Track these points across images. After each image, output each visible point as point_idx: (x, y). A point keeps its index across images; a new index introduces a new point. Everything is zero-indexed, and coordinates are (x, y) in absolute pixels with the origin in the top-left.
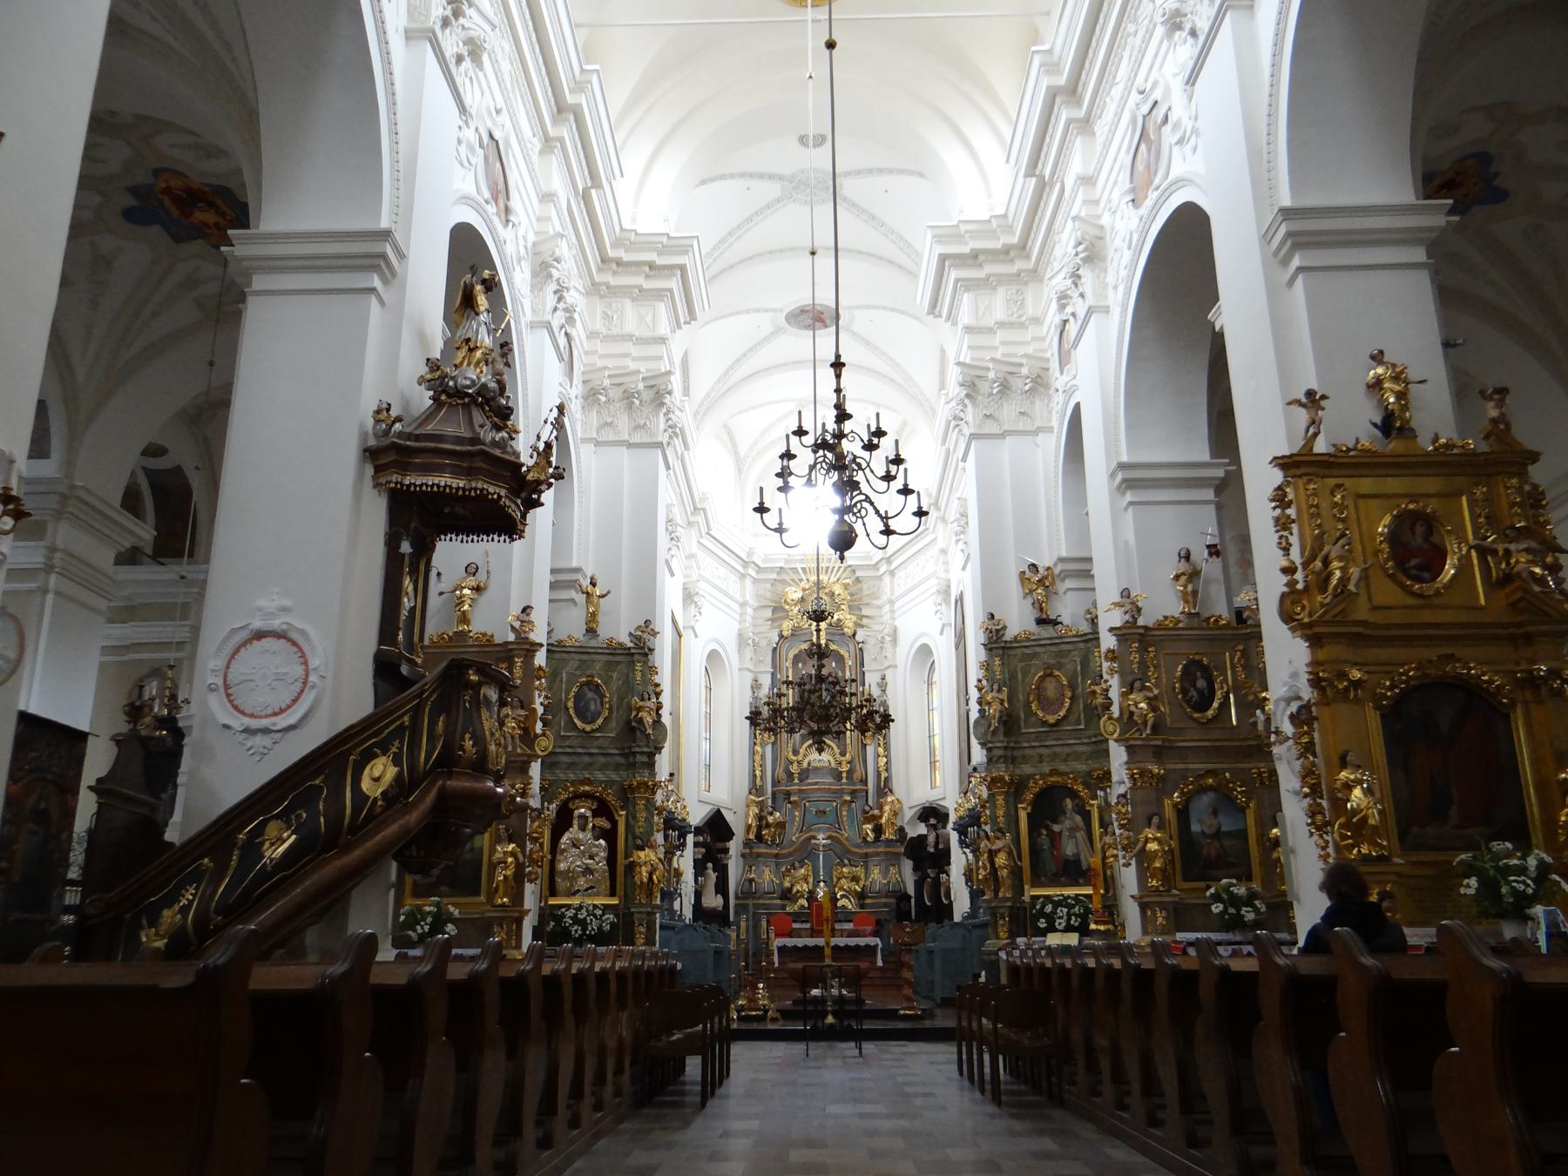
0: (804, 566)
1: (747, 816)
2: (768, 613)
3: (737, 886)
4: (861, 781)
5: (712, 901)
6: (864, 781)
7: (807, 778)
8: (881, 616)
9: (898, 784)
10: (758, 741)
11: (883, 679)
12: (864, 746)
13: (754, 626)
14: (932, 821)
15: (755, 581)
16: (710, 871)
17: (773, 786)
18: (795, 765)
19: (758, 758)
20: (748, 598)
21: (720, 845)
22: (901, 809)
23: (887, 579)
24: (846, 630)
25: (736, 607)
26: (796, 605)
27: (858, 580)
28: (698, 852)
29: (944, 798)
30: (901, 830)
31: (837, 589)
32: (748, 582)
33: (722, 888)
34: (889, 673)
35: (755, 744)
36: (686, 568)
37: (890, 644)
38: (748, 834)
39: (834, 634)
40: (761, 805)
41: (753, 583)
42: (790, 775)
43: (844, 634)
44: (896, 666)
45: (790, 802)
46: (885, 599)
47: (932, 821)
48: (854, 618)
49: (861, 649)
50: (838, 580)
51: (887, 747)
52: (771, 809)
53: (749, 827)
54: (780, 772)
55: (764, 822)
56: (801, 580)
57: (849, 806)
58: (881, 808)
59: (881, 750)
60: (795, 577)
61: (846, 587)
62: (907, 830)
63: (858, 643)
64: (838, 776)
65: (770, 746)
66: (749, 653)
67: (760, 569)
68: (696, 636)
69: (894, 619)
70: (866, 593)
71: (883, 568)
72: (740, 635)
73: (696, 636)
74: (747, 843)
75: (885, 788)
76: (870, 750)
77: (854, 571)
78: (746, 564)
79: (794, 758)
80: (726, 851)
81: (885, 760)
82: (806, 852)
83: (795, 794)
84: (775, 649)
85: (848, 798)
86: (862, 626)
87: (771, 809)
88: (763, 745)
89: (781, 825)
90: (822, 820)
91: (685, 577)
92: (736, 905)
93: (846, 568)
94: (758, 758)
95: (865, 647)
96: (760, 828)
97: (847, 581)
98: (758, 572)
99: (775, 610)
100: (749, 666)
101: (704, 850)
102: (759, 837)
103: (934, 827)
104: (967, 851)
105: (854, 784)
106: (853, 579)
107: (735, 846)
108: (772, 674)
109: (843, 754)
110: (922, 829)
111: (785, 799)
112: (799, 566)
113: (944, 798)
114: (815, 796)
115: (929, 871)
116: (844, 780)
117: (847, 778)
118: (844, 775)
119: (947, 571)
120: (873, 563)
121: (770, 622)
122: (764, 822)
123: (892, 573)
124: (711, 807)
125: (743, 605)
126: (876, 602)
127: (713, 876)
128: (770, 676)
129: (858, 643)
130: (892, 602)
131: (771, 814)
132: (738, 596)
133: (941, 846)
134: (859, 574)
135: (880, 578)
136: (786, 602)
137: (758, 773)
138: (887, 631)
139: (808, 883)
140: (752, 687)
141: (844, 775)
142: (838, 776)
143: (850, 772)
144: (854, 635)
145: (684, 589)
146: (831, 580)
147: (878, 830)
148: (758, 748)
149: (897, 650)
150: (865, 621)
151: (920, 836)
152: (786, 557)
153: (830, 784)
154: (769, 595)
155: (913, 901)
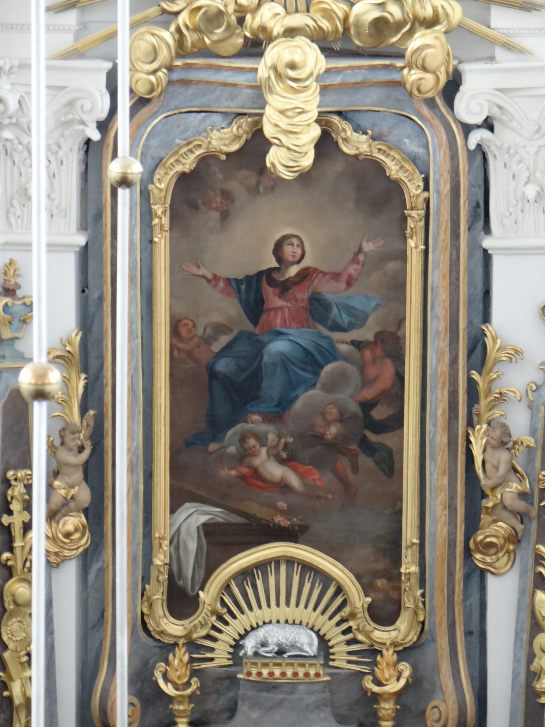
63: (467, 129)
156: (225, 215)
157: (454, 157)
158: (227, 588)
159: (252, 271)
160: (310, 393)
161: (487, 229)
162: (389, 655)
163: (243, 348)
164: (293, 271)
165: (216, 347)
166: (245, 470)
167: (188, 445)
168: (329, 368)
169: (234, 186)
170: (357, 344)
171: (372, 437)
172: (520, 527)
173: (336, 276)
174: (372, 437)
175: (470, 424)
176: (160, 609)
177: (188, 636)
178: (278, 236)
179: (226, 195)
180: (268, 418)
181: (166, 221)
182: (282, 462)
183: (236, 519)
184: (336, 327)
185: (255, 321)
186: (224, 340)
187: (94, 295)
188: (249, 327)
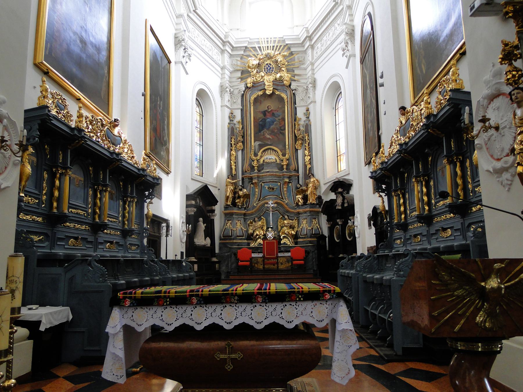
0: (259, 46)
1: (226, 191)
2: (239, 74)
3: (221, 231)
4: (295, 170)
5: (201, 240)
6: (298, 171)
7: (263, 169)
8: (306, 75)
9: (317, 171)
10: (233, 148)
11: (308, 110)
12: (297, 150)
13: (230, 82)
14: (340, 190)
15: (231, 56)
16: (201, 223)
17: (243, 174)
18: (255, 162)
19: (233, 158)
20: (226, 63)
21: (209, 208)
22: (319, 185)
23: (309, 51)
24: (285, 82)
25: (219, 69)
26: (254, 68)
27: (291, 54)
28: (191, 211)
29: (349, 174)
30: (319, 198)
31: (280, 58)
32: (226, 56)
33: (209, 232)
34: (311, 107)
35: (231, 150)
36: (177, 24)
37: (312, 88)
38: (227, 202)
39: (278, 85)
40: (235, 184)
41: (230, 58)
42: (252, 168)
43: (284, 85)
44: (315, 102)
45: (252, 184)
46: (309, 62)
47: (340, 190)
48: (289, 76)
49: (294, 94)
50: (280, 54)
51: (310, 150)
52: (240, 187)
53: (227, 198)
54: (246, 165)
55: (237, 195)
56: (258, 55)
57: (288, 185)
58: (307, 185)
59: (307, 152)
60: (256, 54)
61: (284, 56)
62: (323, 198)
64: (281, 168)
65: (240, 152)
66: (227, 97)
67: (233, 48)
68: (187, 73)
69: (314, 74)
70: (296, 60)
71: (307, 44)
72: (221, 86)
73: (187, 73)
74: (227, 207)
75: (309, 174)
76: (300, 152)
77: (289, 49)
78: (224, 43)
79: (254, 158)
80: (213, 211)
81: (309, 157)
82: (262, 213)
83: (255, 178)
84: (243, 96)
85: (287, 180)
86: (295, 81)
87: (240, 187)
88: (237, 151)
89: (247, 196)
90: (272, 193)
91: (176, 30)
92: (220, 243)
93: (285, 46)
94: (233, 158)
95: (297, 94)
96: (234, 198)
97: (285, 53)
98: (232, 50)
99: (243, 72)
100: (228, 104)
101: (195, 209)
102: (234, 204)
103: (341, 193)
104: (383, 194)
105: (290, 172)
106: (289, 52)
107: (218, 209)
108: (242, 110)
109: (284, 155)
110: (333, 196)
111: (249, 182)
112: (257, 46)
113: (349, 174)
114: (267, 179)
115: (338, 220)
116: (285, 170)
117: (287, 169)
118: (285, 167)
119: (352, 20)
120: (301, 42)
121: (240, 80)
122: (237, 195)
123: (312, 47)
124: (202, 184)
125: (223, 68)
126: (302, 66)
127: (202, 226)
128: (240, 111)
129: (293, 91)
130: (312, 64)
131: (241, 190)
132: (220, 63)
133: (346, 205)
134: (293, 50)
135: (305, 52)
136: (249, 67)
137: (233, 167)
138: (310, 80)
139: (263, 230)
140: (229, 117)
141: (285, 167)
142: (281, 168)
143: (288, 165)
144: (290, 85)
145: (176, 38)
146: (276, 53)
147: (305, 198)
148: (233, 152)
149: (316, 92)
150: (296, 78)
151: (331, 200)
152: (248, 39)
153: (276, 172)
154: (239, 63)
155: (327, 239)
156: (261, 103)
157: (291, 93)
158: (262, 153)
159: (264, 110)
160: (273, 126)
161: (296, 104)
162: (285, 160)
163: (263, 120)
164: (270, 110)
165: (260, 120)
166: (264, 137)
167: (256, 133)
168: (275, 122)
169: (262, 100)
170: (279, 119)
171: (281, 131)
172: (302, 142)
173: (276, 110)
174: (281, 131)
175: (295, 129)
176: (253, 155)
177: (256, 159)
178: (267, 106)
179: (261, 101)
180: (267, 130)
181: (253, 104)
182: (269, 135)
183: (263, 143)
184: (276, 117)
185: (265, 117)
186: (261, 119)
187: (243, 116)
188: (264, 118)
